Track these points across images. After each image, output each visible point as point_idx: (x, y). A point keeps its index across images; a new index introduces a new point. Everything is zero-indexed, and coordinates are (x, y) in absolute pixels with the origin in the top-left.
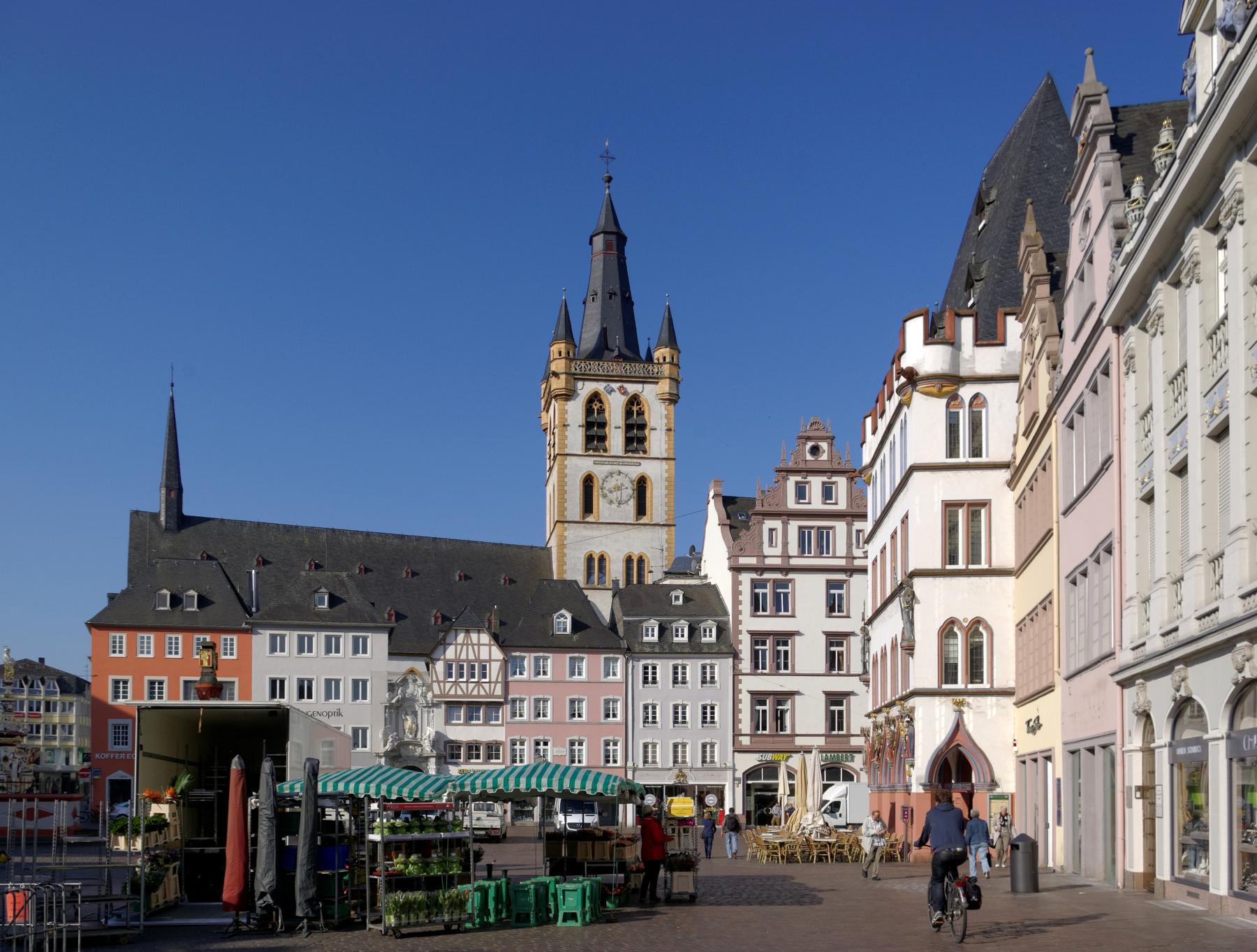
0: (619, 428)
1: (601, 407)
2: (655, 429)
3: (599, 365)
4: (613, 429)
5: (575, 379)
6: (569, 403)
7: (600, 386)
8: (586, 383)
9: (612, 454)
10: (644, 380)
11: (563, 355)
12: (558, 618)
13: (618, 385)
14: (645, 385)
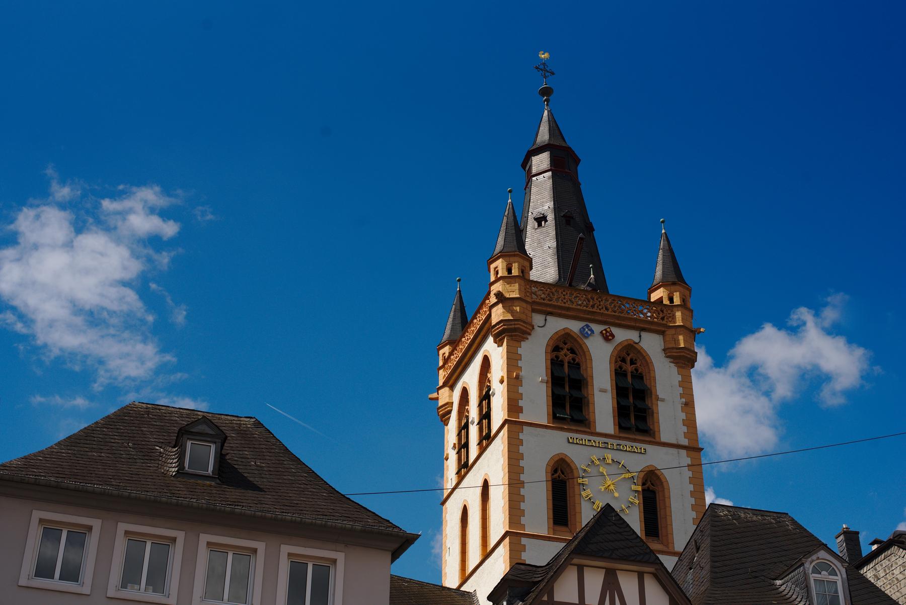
0: (603, 391)
1: (574, 359)
2: (663, 400)
3: (571, 294)
4: (596, 392)
5: (534, 311)
6: (523, 343)
7: (575, 326)
8: (549, 318)
9: (598, 430)
10: (642, 327)
11: (515, 272)
12: (816, 571)
13: (602, 328)
14: (644, 334)
